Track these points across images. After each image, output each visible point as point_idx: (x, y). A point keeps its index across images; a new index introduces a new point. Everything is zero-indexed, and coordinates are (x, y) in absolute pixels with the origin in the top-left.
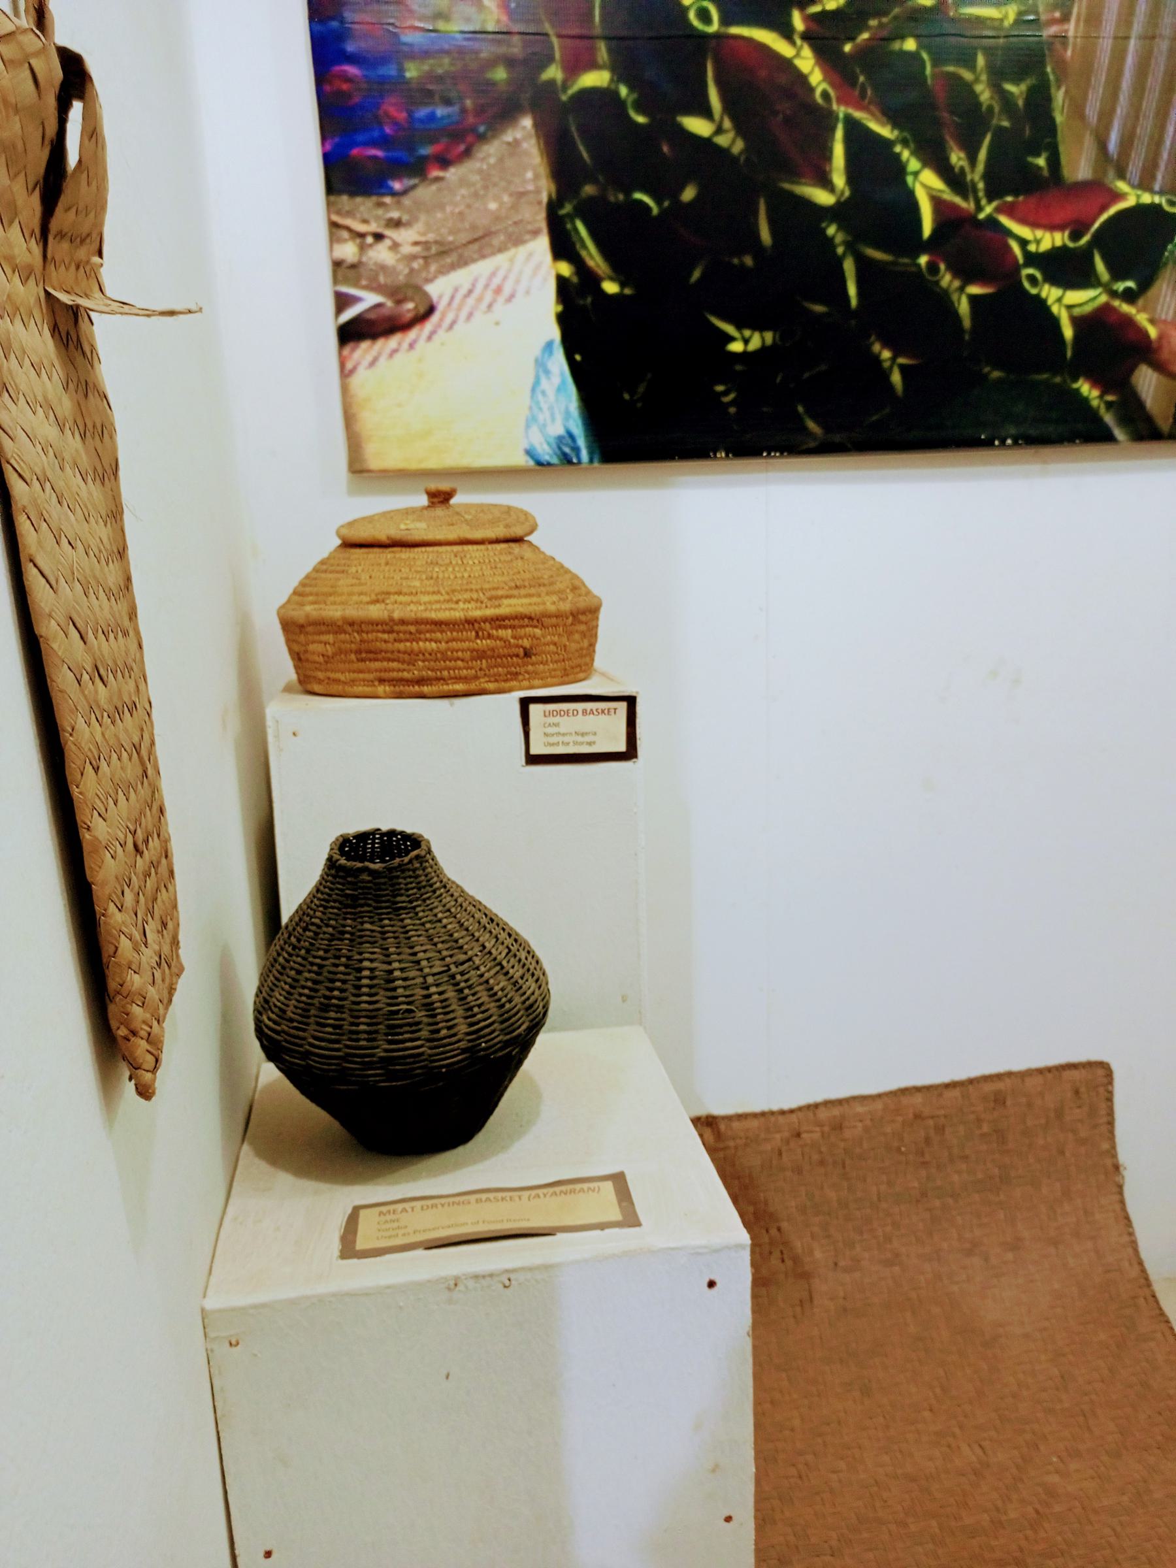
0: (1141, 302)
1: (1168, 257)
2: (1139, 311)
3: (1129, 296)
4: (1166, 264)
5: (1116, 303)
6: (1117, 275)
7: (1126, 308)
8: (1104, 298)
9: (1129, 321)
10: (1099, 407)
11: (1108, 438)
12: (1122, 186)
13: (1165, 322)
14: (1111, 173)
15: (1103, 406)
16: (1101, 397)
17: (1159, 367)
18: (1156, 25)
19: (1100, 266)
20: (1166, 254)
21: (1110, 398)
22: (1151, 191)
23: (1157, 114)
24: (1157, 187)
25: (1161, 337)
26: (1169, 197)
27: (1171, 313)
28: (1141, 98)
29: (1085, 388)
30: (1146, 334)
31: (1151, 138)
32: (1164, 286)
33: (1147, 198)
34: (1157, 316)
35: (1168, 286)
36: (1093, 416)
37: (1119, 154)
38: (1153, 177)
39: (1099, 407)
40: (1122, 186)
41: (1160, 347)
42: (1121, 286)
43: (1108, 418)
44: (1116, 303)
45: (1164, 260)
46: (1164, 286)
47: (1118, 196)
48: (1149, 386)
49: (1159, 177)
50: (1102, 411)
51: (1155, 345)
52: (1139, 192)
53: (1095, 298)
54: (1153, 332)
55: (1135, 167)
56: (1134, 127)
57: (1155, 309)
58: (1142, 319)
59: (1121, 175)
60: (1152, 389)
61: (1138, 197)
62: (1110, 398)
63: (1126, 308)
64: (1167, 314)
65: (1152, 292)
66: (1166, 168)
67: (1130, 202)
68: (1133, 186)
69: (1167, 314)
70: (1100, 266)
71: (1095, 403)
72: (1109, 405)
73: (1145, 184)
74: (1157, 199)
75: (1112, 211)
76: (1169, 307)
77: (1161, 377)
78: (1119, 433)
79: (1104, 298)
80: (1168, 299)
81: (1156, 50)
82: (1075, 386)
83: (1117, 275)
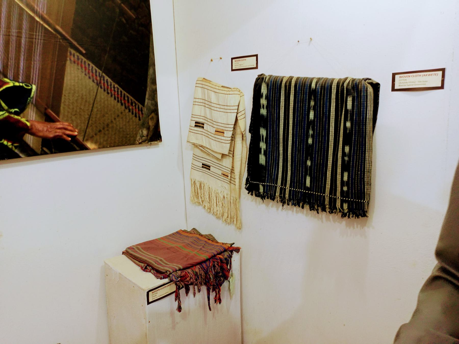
0: (22, 115)
1: (29, 102)
2: (21, 118)
3: (16, 113)
4: (29, 104)
5: (12, 116)
6: (10, 107)
7: (16, 117)
8: (7, 114)
9: (19, 121)
10: (12, 148)
11: (18, 157)
12: (6, 80)
13: (32, 120)
14: (2, 76)
15: (13, 147)
16: (12, 145)
17: (33, 134)
18: (9, 32)
19: (3, 104)
20: (28, 101)
21: (16, 145)
22: (19, 82)
23: (15, 59)
24: (20, 81)
25: (31, 125)
26: (25, 84)
27: (34, 118)
28: (8, 54)
29: (5, 143)
30: (26, 125)
31: (15, 66)
32: (30, 110)
33: (17, 84)
34: (29, 119)
35: (31, 110)
36: (11, 150)
37: (3, 70)
38: (19, 78)
39: (12, 148)
40: (6, 80)
41: (32, 128)
42: (13, 110)
43: (16, 151)
44: (12, 116)
45: (28, 102)
46: (30, 110)
47: (6, 83)
48: (30, 140)
49: (21, 78)
50: (14, 149)
51: (30, 128)
52: (14, 82)
53: (3, 114)
54: (28, 124)
55: (10, 74)
56: (7, 63)
57: (28, 117)
58: (23, 120)
59: (6, 77)
60: (32, 141)
61: (14, 83)
62: (16, 145)
63: (16, 117)
64: (32, 118)
65: (25, 112)
66: (22, 74)
67: (11, 84)
68: (11, 80)
69: (32, 118)
70: (3, 104)
71: (10, 147)
72: (16, 147)
73: (15, 79)
74: (21, 84)
75: (4, 87)
76: (33, 116)
77: (34, 137)
78: (21, 155)
79: (7, 114)
80: (32, 114)
81: (11, 40)
82: (1, 142)
83: (10, 107)
